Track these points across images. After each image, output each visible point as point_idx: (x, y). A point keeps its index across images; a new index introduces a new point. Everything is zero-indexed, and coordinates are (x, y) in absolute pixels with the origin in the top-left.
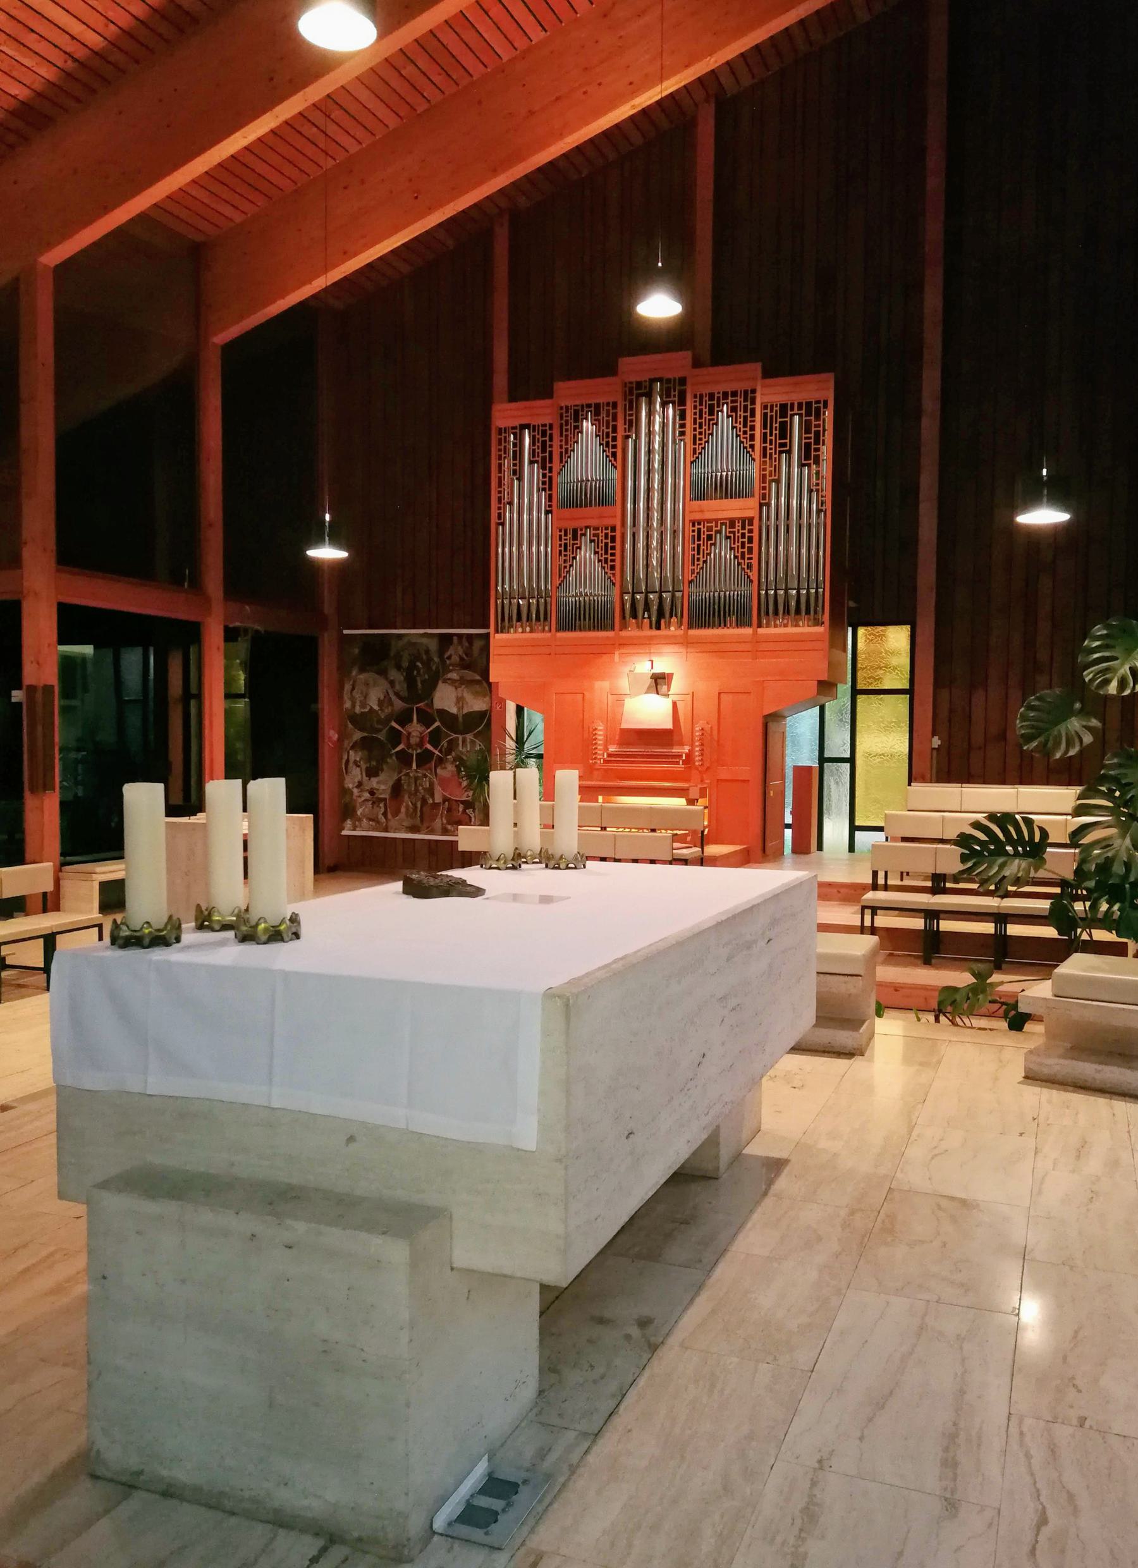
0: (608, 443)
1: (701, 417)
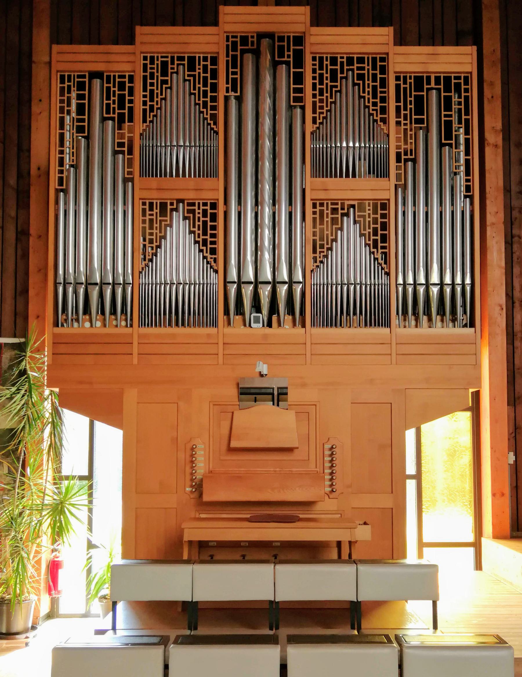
0: (205, 104)
1: (321, 83)
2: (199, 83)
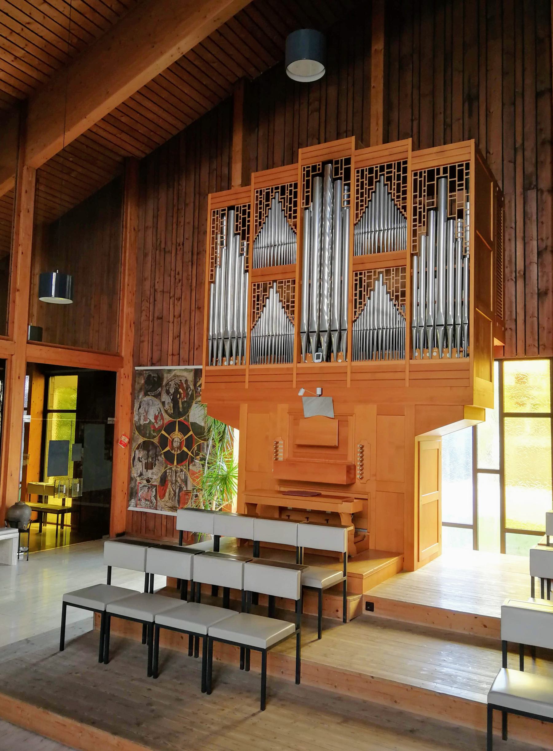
1: (362, 188)
2: (287, 203)
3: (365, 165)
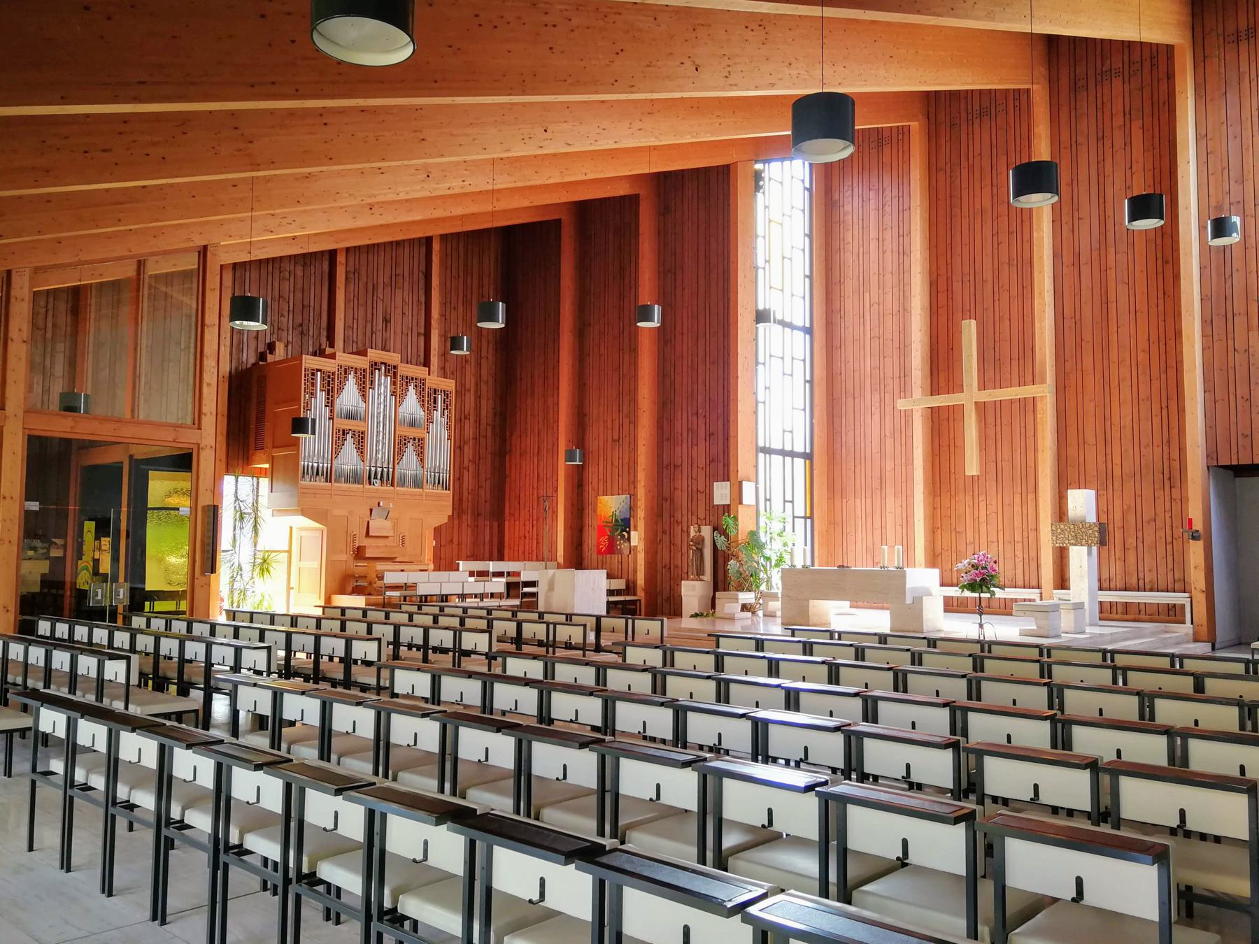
3: (405, 374)
